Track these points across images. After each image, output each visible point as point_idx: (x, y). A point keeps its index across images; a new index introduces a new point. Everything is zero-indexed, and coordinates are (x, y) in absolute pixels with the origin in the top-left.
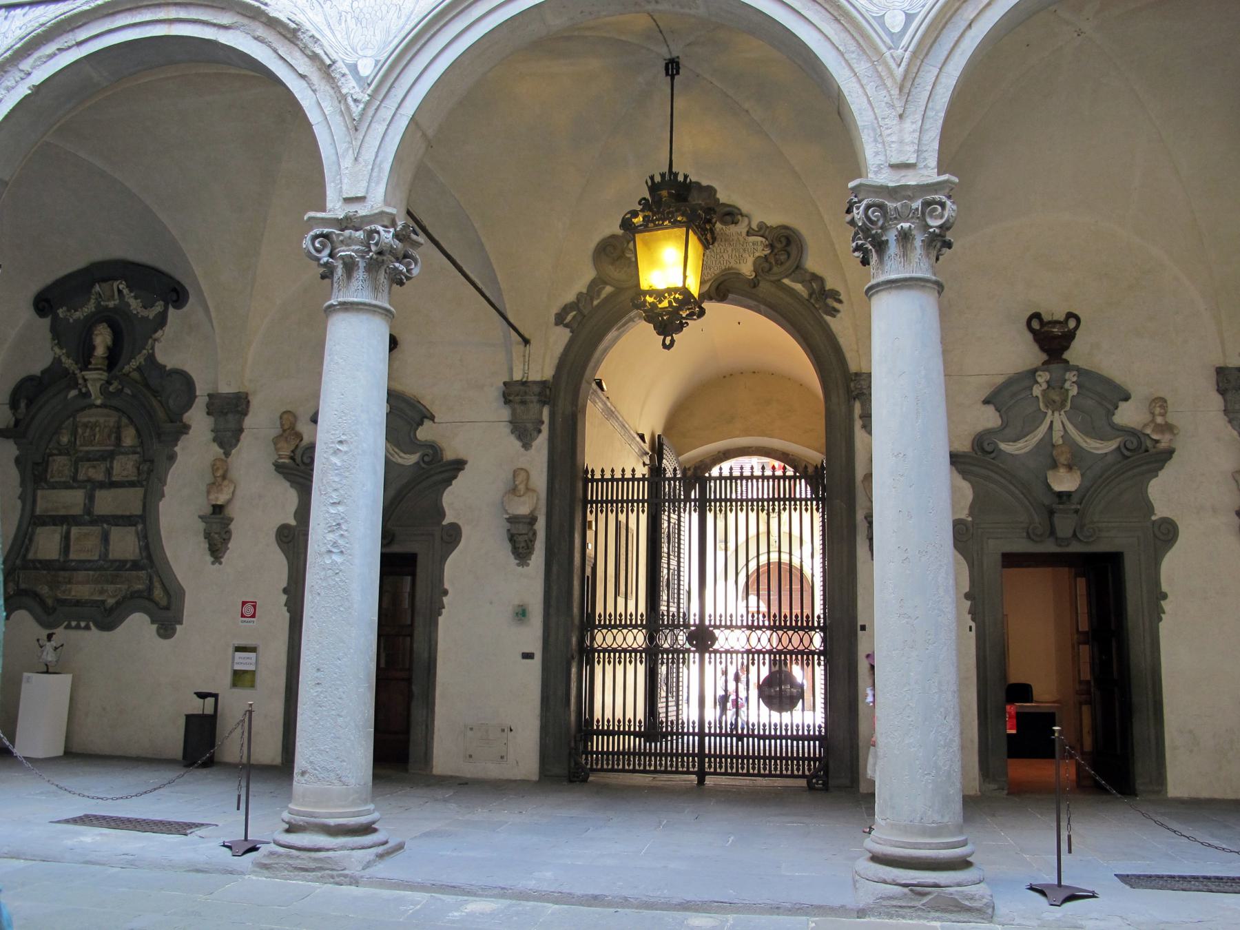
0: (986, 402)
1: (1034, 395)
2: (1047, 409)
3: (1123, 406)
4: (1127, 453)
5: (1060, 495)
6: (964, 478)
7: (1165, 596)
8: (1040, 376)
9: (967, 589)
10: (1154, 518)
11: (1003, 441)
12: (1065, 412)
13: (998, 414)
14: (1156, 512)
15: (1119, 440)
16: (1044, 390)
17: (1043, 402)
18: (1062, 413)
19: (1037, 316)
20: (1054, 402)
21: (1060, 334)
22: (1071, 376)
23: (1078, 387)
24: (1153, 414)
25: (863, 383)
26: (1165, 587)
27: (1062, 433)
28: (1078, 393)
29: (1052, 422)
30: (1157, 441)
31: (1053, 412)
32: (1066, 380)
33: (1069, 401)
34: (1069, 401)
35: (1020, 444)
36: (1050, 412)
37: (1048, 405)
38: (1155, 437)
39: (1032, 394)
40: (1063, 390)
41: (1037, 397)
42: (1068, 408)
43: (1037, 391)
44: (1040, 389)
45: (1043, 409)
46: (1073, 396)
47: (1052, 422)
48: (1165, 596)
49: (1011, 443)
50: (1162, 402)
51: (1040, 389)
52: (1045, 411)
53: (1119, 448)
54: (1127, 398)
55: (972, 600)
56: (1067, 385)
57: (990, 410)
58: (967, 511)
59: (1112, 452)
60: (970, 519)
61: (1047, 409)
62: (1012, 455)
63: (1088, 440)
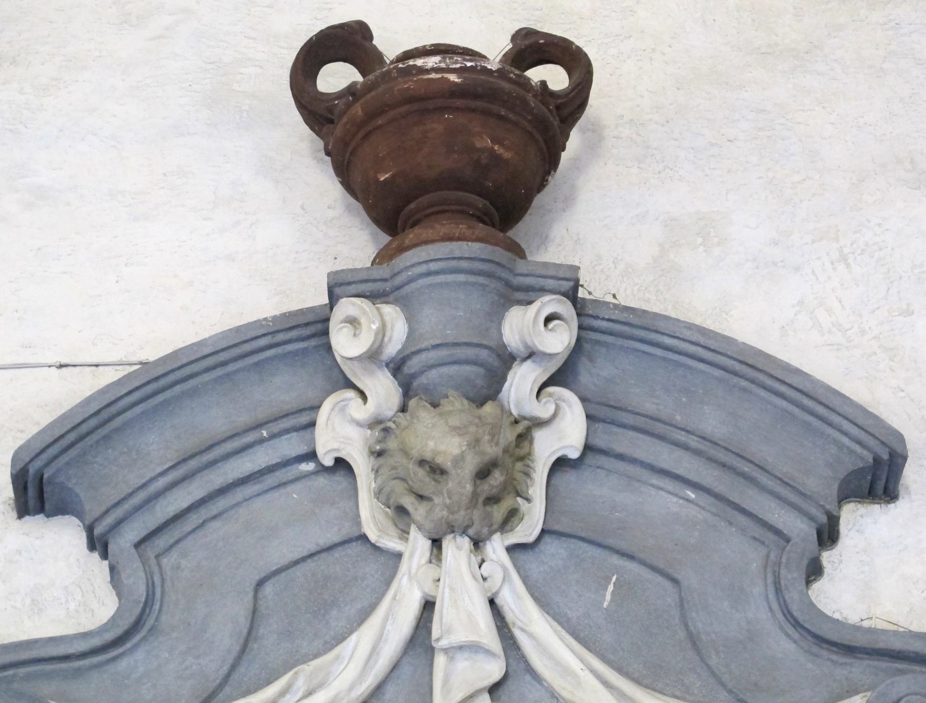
1: (328, 462)
2: (404, 534)
8: (353, 322)
12: (512, 549)
13: (98, 567)
16: (376, 423)
18: (496, 547)
20: (436, 471)
21: (453, 78)
23: (590, 418)
27: (494, 670)
28: (588, 448)
29: (428, 606)
31: (436, 543)
33: (538, 490)
34: (538, 490)
36: (419, 544)
37: (408, 502)
39: (312, 455)
41: (342, 465)
42: (527, 531)
44: (360, 411)
46: (561, 464)
47: (428, 606)
51: (360, 411)
52: (391, 543)
61: (404, 534)
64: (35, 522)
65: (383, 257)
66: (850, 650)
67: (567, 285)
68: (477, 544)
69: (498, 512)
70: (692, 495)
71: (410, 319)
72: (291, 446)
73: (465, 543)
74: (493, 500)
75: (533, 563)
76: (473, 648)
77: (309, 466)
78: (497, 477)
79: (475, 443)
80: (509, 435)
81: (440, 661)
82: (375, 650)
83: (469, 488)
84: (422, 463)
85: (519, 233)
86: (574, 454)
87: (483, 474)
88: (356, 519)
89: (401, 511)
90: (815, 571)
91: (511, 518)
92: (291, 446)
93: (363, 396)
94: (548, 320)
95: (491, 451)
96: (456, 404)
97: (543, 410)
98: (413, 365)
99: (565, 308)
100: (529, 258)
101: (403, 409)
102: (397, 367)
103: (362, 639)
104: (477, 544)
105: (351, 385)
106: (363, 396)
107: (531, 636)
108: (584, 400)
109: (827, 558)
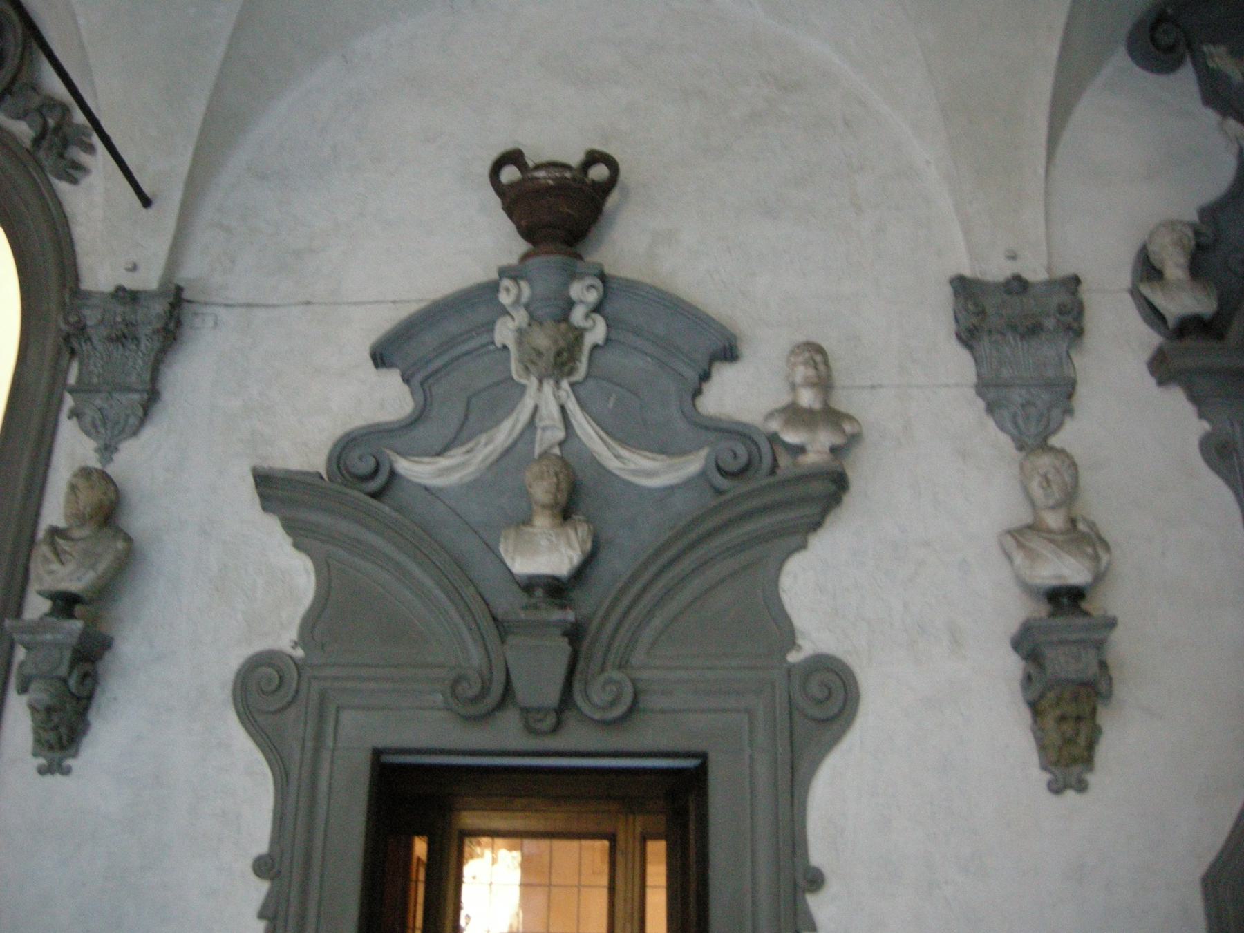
0: (380, 357)
2: (528, 379)
3: (724, 375)
4: (720, 481)
5: (529, 585)
6: (297, 546)
7: (816, 881)
8: (507, 290)
9: (262, 847)
10: (793, 657)
11: (404, 455)
12: (572, 385)
14: (800, 641)
15: (704, 452)
17: (521, 361)
18: (565, 384)
19: (513, 157)
20: (539, 354)
21: (551, 182)
22: (584, 293)
23: (608, 325)
24: (793, 387)
25: (87, 312)
26: (818, 855)
27: (560, 434)
28: (608, 340)
30: (800, 450)
31: (541, 382)
32: (571, 304)
35: (444, 462)
36: (533, 382)
37: (529, 365)
38: (791, 437)
39: (493, 343)
40: (563, 326)
41: (505, 347)
43: (505, 332)
44: (512, 325)
45: (515, 377)
46: (595, 347)
47: (536, 409)
48: (816, 881)
49: (426, 459)
50: (814, 352)
52: (523, 381)
53: (703, 474)
54: (729, 353)
55: (272, 879)
56: (578, 316)
57: (392, 378)
58: (293, 634)
59: (687, 484)
60: (299, 653)
62: (426, 488)
63: (624, 452)
64: (383, 371)
65: (525, 257)
66: (707, 428)
67: (596, 271)
68: (557, 383)
69: (566, 369)
70: (649, 359)
71: (532, 287)
72: (484, 339)
73: (552, 382)
74: (563, 364)
75: (582, 392)
76: (553, 427)
77: (492, 347)
78: (565, 355)
79: (556, 341)
80: (571, 336)
81: (539, 432)
82: (514, 426)
83: (552, 360)
84: (534, 349)
85: (580, 249)
86: (600, 342)
87: (559, 354)
88: (509, 371)
89: (527, 368)
90: (697, 392)
91: (571, 372)
92: (484, 339)
93: (513, 318)
94: (592, 286)
95: (562, 344)
96: (549, 324)
97: (588, 324)
98: (531, 308)
99: (598, 283)
100: (585, 260)
101: (530, 325)
102: (527, 307)
103: (506, 425)
104: (557, 383)
105: (508, 313)
106: (513, 318)
107: (575, 420)
108: (606, 318)
109: (706, 387)
